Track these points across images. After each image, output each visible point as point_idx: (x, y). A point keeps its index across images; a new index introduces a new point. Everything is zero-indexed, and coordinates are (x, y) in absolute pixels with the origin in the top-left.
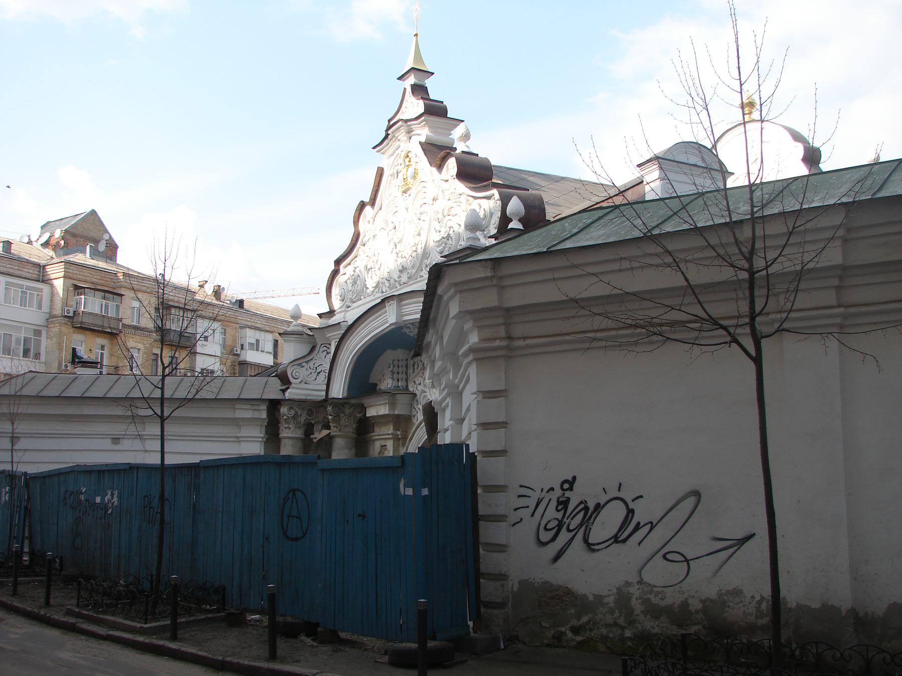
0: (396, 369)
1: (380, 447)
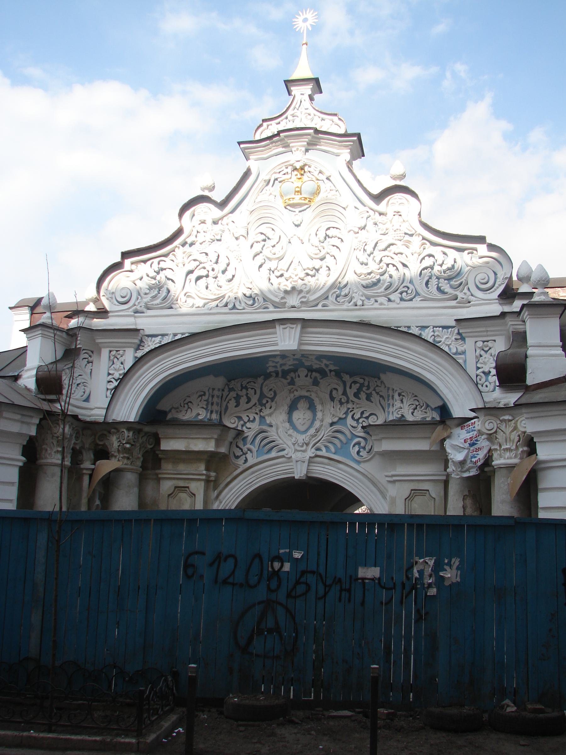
0: (210, 399)
1: (173, 488)
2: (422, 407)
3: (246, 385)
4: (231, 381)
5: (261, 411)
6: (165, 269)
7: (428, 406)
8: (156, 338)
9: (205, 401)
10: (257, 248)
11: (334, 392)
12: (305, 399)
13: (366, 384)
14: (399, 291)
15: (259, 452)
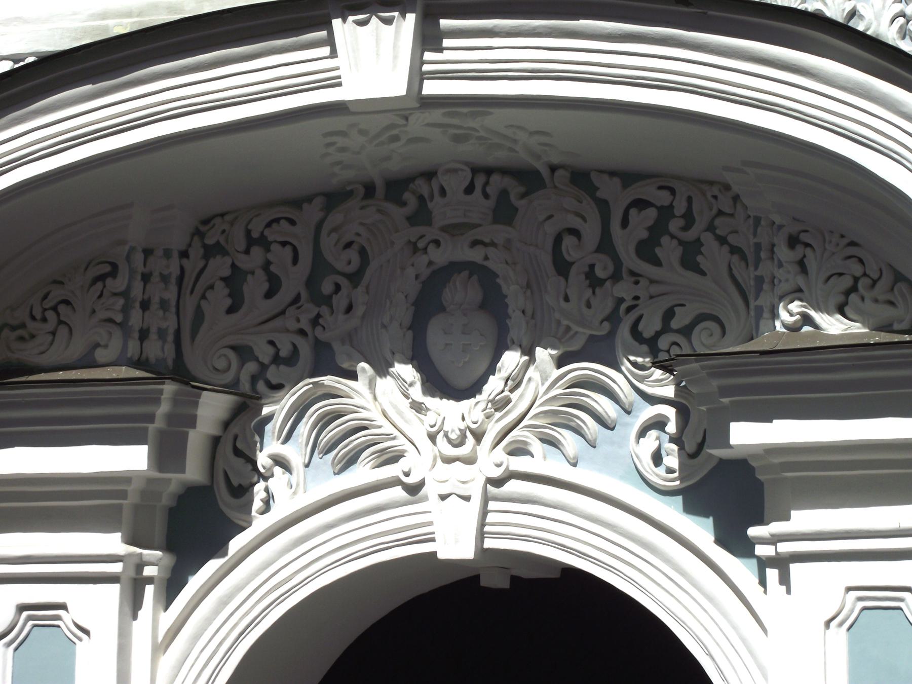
0: (138, 285)
3: (262, 233)
4: (212, 222)
13: (680, 208)
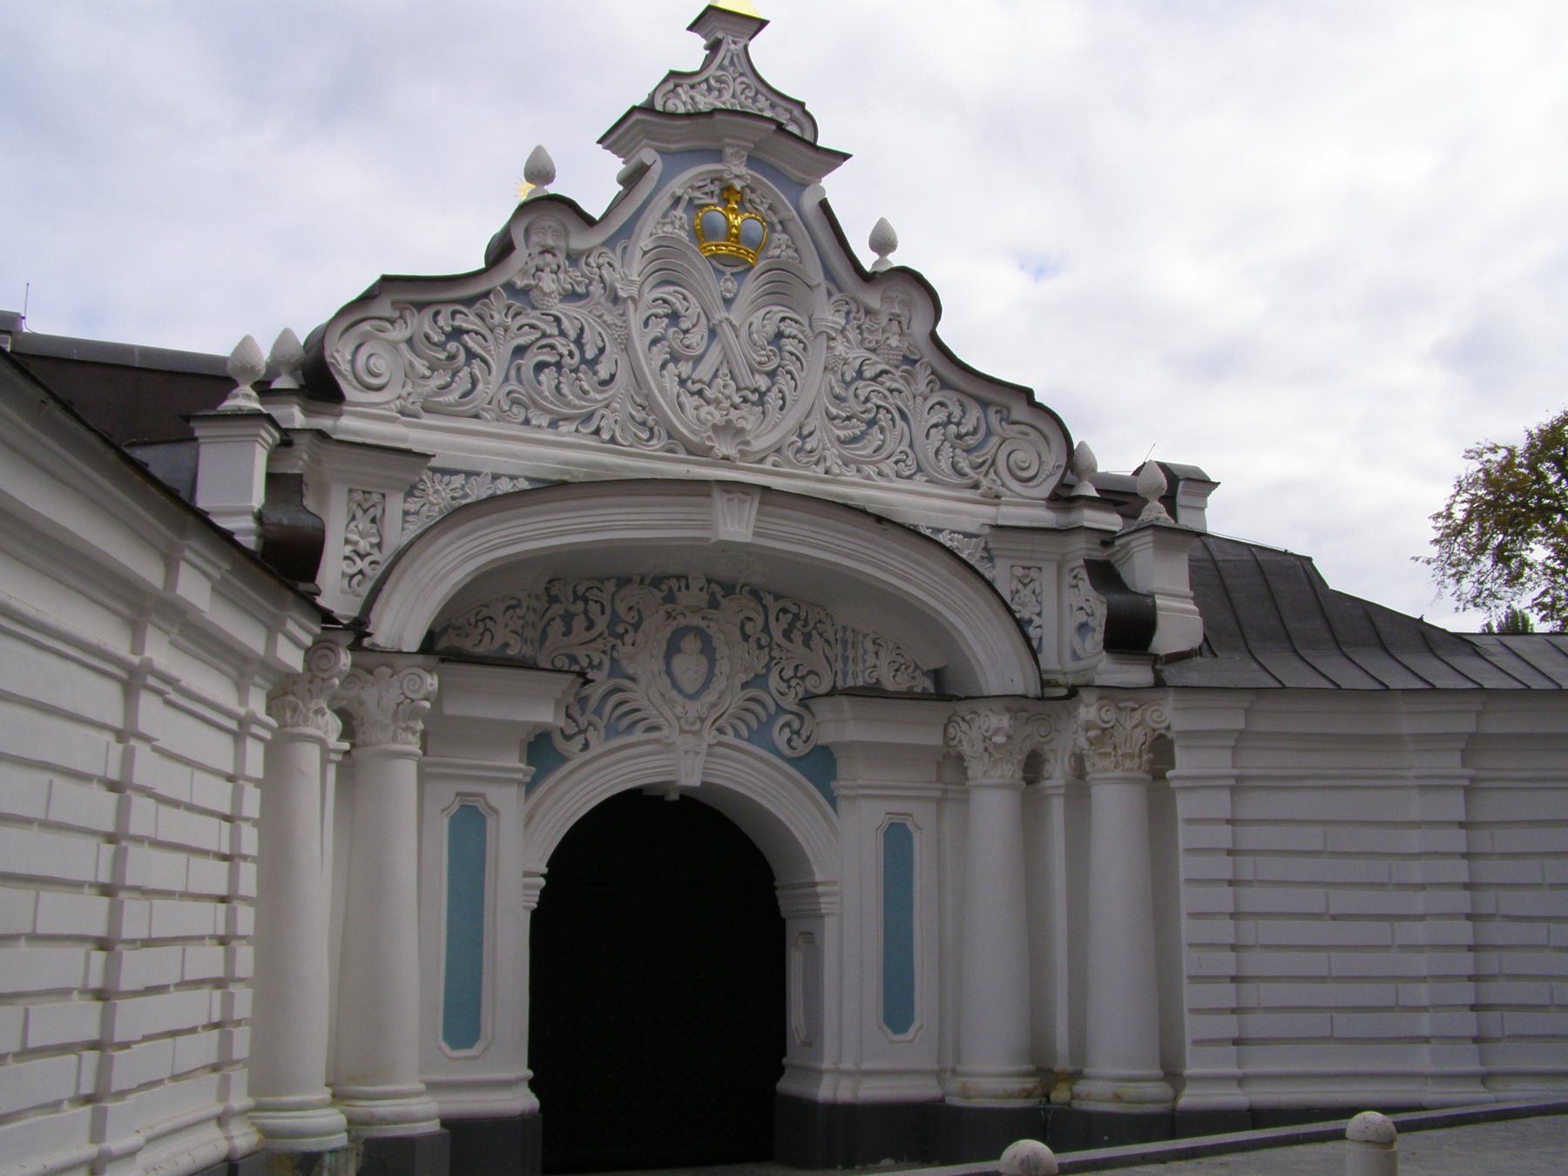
2: (906, 669)
3: (584, 594)
5: (613, 647)
6: (467, 332)
7: (917, 667)
8: (452, 478)
9: (519, 618)
10: (657, 328)
11: (749, 627)
12: (693, 633)
13: (803, 615)
14: (894, 459)
15: (611, 732)
